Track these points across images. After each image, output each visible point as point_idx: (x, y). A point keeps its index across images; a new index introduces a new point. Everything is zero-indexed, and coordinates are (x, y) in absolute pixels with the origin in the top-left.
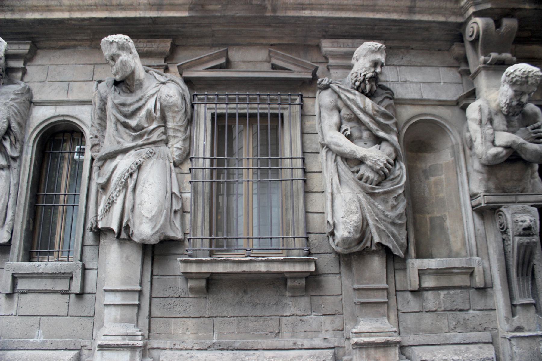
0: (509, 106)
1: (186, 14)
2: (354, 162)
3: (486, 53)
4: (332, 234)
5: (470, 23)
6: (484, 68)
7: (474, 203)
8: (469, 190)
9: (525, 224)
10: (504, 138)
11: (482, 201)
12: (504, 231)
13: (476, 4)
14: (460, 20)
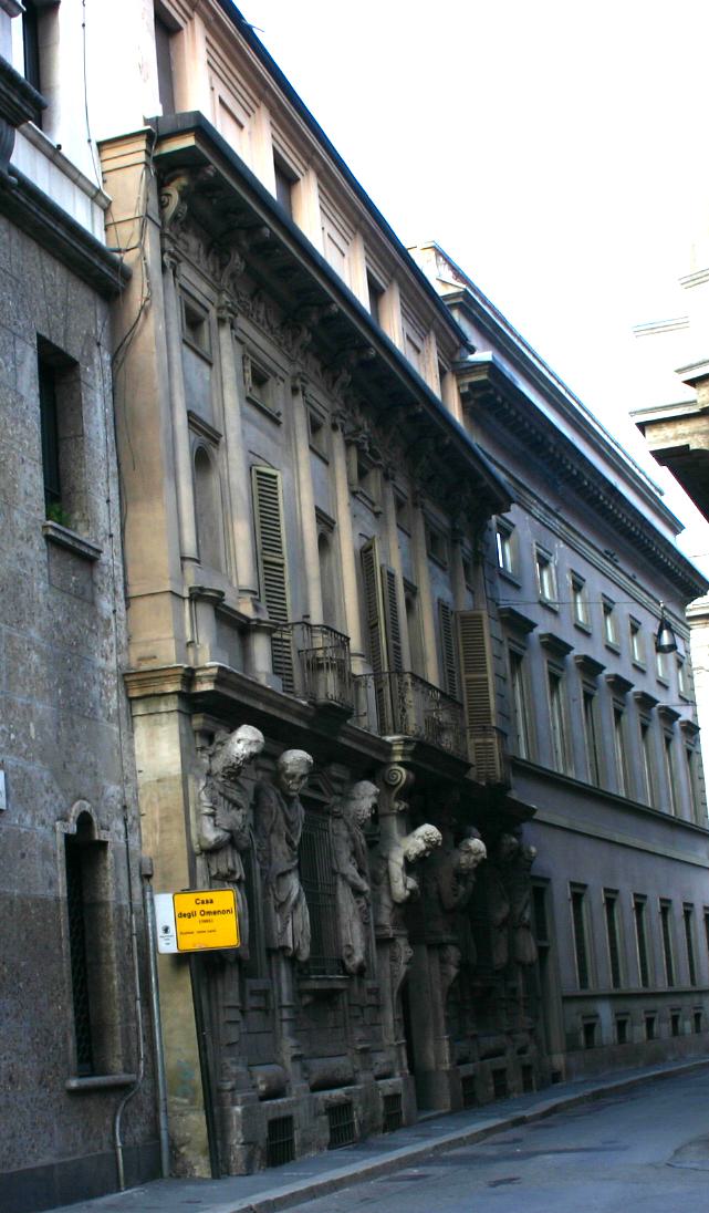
0: (417, 856)
1: (303, 725)
2: (357, 892)
3: (398, 798)
4: (349, 957)
5: (393, 768)
6: (397, 815)
7: (381, 933)
8: (375, 920)
9: (411, 955)
10: (412, 883)
11: (391, 932)
12: (394, 959)
13: (403, 755)
14: (383, 759)
